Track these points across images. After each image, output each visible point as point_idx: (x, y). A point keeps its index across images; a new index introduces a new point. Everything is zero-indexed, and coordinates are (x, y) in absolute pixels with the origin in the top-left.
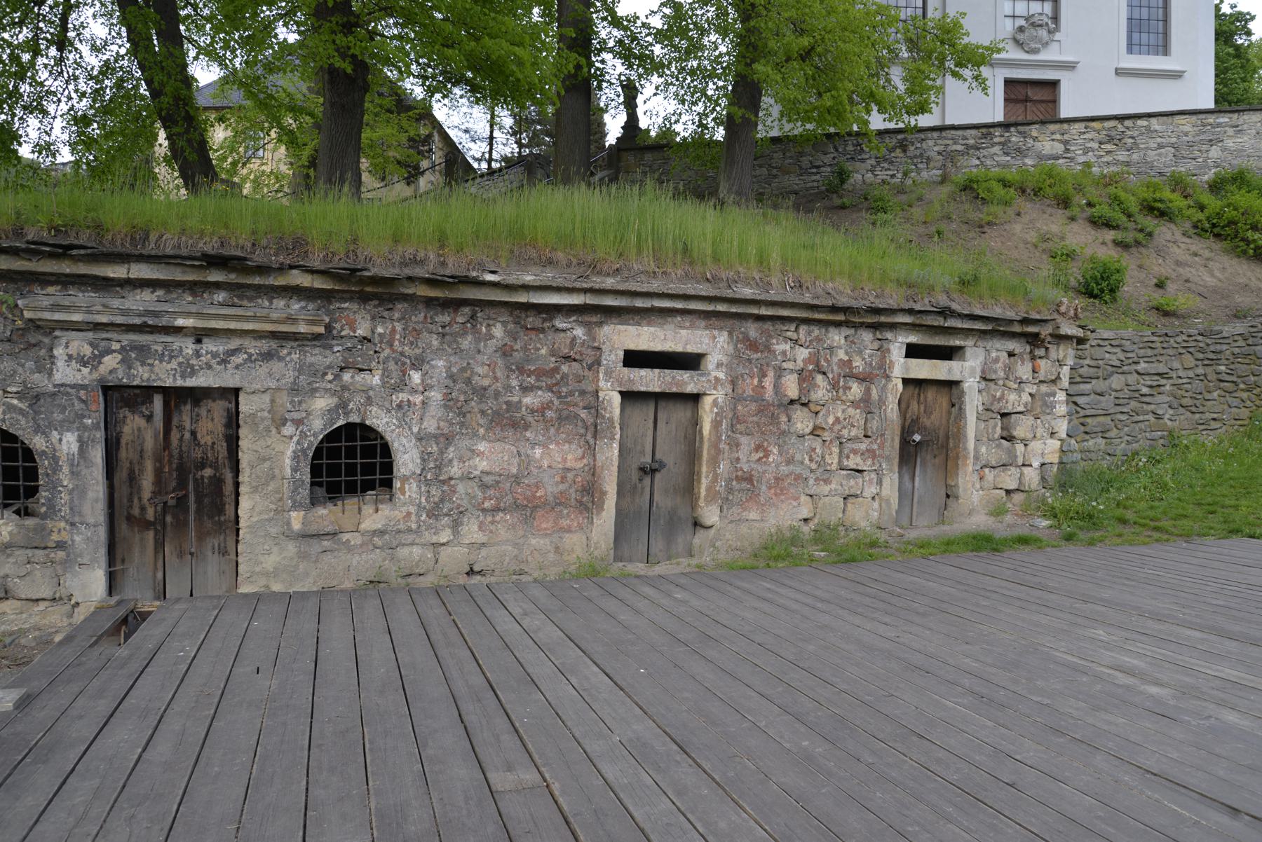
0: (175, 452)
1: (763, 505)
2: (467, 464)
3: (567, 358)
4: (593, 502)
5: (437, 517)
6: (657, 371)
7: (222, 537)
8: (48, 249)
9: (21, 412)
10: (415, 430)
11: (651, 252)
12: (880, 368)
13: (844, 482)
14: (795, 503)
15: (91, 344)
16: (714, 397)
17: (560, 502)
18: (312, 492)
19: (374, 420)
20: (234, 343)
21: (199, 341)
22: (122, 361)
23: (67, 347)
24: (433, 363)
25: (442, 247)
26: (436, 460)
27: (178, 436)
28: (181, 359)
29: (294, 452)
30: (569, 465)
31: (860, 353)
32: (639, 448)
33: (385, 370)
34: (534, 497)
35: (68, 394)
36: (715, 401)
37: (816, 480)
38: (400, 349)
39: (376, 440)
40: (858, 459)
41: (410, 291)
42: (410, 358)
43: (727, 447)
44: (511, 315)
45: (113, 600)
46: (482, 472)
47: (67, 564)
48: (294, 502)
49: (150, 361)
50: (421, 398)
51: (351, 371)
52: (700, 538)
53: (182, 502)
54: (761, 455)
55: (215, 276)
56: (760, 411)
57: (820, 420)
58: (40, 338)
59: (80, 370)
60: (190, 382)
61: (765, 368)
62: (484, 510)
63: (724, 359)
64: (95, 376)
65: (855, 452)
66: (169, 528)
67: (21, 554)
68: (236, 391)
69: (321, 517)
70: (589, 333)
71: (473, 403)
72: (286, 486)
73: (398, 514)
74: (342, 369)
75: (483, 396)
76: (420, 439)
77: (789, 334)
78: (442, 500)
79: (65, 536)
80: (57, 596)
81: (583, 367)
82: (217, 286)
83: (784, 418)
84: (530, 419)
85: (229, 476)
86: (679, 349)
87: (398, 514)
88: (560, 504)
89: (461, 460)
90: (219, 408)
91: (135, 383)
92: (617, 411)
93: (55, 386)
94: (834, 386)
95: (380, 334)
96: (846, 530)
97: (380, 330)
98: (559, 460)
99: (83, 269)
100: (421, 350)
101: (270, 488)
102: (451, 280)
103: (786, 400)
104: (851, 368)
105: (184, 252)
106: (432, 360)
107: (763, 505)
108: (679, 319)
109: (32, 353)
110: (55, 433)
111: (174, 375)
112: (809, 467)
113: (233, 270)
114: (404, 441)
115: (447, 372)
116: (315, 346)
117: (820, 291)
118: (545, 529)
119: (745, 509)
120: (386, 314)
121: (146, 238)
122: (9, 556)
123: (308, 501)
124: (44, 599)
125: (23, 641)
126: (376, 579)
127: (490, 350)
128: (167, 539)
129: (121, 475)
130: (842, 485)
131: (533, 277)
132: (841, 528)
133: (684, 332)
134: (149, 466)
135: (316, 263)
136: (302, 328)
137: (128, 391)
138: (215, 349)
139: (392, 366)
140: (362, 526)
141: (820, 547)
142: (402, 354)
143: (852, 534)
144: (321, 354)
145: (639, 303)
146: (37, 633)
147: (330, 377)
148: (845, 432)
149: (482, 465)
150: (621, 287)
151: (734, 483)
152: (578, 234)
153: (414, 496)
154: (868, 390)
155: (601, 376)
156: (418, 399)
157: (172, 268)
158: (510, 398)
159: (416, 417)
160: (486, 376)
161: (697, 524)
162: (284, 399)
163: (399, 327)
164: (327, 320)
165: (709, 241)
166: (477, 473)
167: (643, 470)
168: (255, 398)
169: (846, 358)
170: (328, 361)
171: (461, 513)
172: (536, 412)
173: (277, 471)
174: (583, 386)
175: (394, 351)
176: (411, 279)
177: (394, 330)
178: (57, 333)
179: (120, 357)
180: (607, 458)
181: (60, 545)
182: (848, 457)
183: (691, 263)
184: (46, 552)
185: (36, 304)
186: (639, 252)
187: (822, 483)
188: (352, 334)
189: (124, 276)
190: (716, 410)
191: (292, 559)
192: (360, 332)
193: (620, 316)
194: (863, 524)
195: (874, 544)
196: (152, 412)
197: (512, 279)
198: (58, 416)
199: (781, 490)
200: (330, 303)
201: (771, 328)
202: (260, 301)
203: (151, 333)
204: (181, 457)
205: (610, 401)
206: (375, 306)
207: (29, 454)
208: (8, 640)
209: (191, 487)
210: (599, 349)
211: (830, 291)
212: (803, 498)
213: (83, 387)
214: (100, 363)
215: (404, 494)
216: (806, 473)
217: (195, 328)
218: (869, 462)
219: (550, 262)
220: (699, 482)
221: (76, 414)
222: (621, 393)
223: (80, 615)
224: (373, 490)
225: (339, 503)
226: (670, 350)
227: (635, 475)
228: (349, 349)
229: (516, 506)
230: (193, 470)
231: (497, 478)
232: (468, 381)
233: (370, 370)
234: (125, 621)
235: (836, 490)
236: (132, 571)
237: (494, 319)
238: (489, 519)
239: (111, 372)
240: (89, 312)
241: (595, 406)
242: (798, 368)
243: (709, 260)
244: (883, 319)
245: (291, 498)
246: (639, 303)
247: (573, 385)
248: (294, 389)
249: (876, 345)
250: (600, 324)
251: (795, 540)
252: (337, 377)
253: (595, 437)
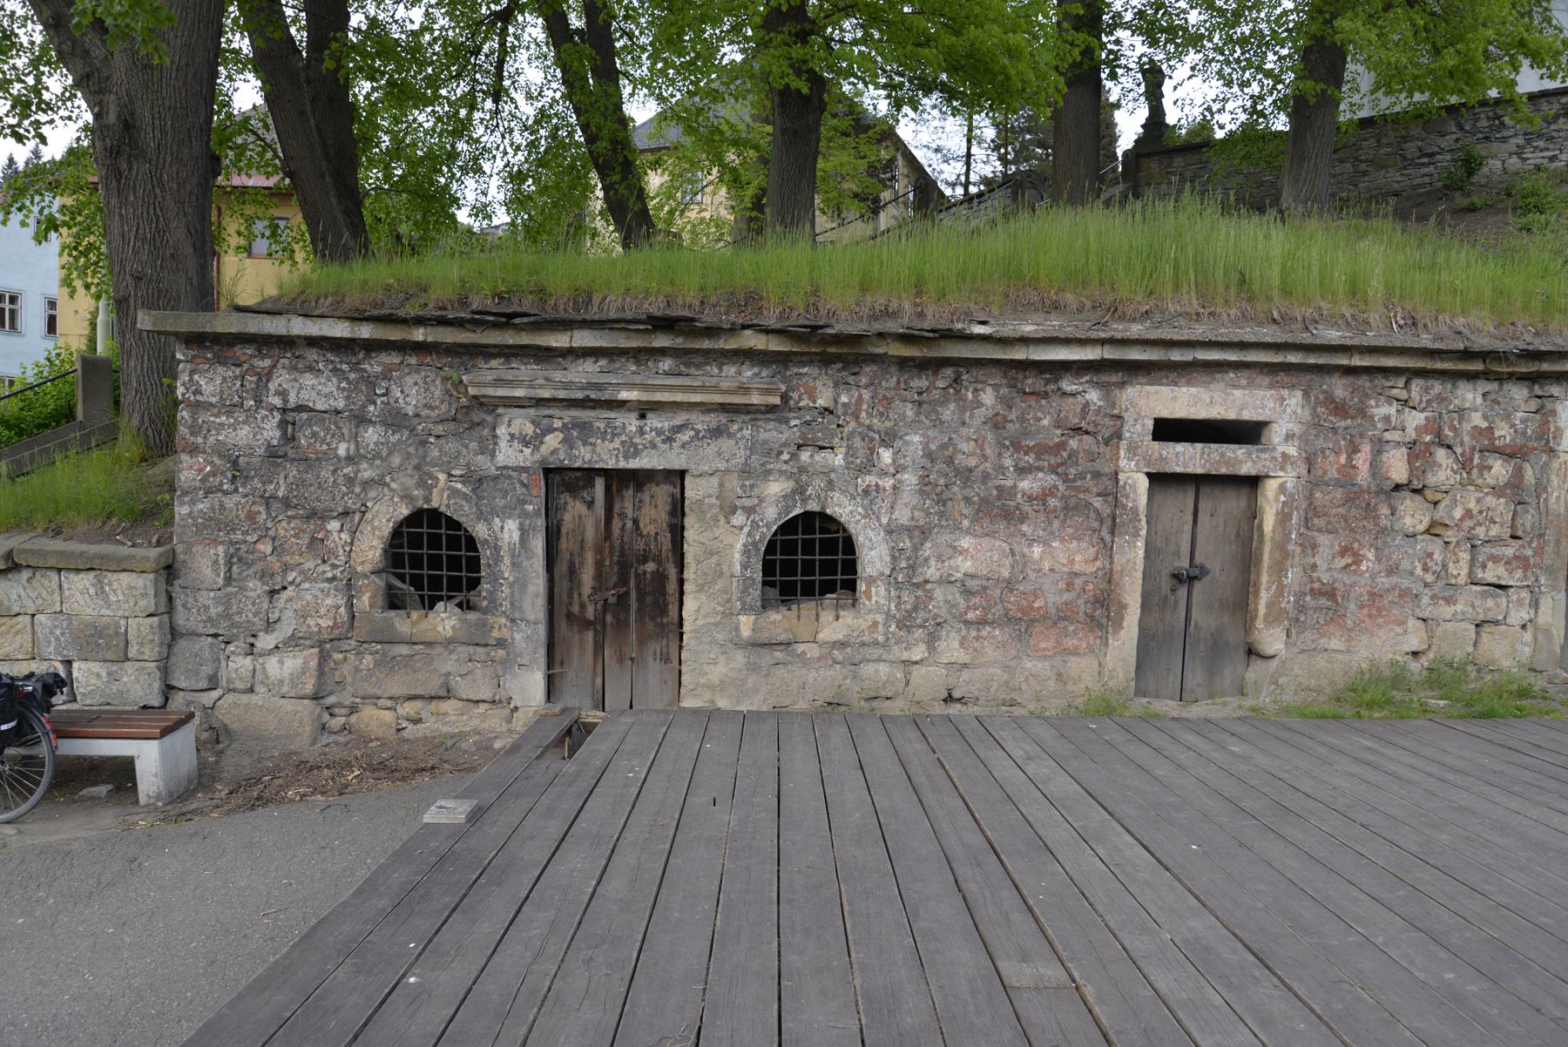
0: (617, 543)
1: (1350, 630)
2: (946, 564)
3: (1077, 430)
4: (1108, 617)
5: (909, 629)
6: (1199, 446)
7: (664, 642)
8: (492, 318)
9: (465, 497)
10: (884, 520)
11: (1193, 285)
12: (1539, 438)
13: (1477, 602)
14: (1398, 630)
15: (533, 422)
16: (1280, 481)
17: (1064, 615)
18: (762, 591)
19: (836, 509)
20: (680, 418)
21: (643, 417)
22: (564, 441)
23: (509, 426)
24: (907, 438)
25: (919, 293)
26: (909, 558)
27: (620, 525)
28: (624, 438)
29: (744, 545)
30: (1077, 568)
31: (1507, 416)
32: (1172, 548)
33: (849, 447)
34: (1032, 608)
35: (510, 477)
36: (1282, 488)
37: (1432, 598)
38: (867, 422)
39: (838, 532)
40: (1501, 570)
41: (880, 351)
42: (879, 432)
43: (1299, 549)
44: (1005, 376)
45: (557, 708)
46: (965, 575)
47: (507, 663)
48: (744, 604)
49: (592, 440)
50: (892, 481)
51: (810, 448)
52: (1255, 672)
53: (623, 599)
54: (1349, 561)
55: (662, 341)
56: (1348, 500)
57: (1441, 513)
58: (484, 416)
59: (522, 451)
60: (634, 464)
61: (1357, 440)
62: (966, 622)
63: (1297, 429)
64: (537, 457)
65: (1495, 559)
66: (609, 629)
67: (463, 651)
68: (682, 474)
69: (774, 623)
70: (1107, 397)
71: (955, 489)
72: (735, 585)
73: (863, 623)
74: (799, 447)
75: (968, 479)
76: (890, 532)
77: (1395, 392)
78: (916, 608)
79: (505, 633)
80: (497, 698)
81: (1098, 442)
82: (663, 352)
83: (1384, 510)
84: (1027, 508)
85: (672, 572)
86: (1231, 415)
87: (863, 623)
88: (1065, 618)
89: (940, 558)
90: (662, 494)
91: (576, 465)
92: (1143, 500)
93: (498, 468)
94: (1465, 465)
95: (844, 405)
96: (1479, 671)
97: (844, 399)
98: (1065, 561)
99: (525, 339)
100: (892, 422)
101: (717, 587)
102: (931, 335)
103: (1388, 485)
104: (1492, 439)
105: (629, 315)
106: (906, 434)
107: (1350, 630)
108: (1232, 375)
109: (476, 432)
110: (497, 520)
111: (617, 456)
112: (1422, 580)
113: (681, 333)
114: (871, 534)
115: (923, 449)
116: (769, 420)
117: (1445, 329)
118: (1045, 649)
119: (1323, 635)
120: (851, 379)
121: (589, 301)
122: (451, 652)
123: (759, 604)
124: (484, 701)
125: (464, 745)
126: (836, 701)
127: (977, 422)
128: (607, 641)
129: (562, 567)
130: (1473, 606)
131: (1035, 327)
132: (1470, 668)
133: (1238, 393)
134: (590, 558)
135: (772, 322)
136: (756, 399)
137: (570, 473)
138: (659, 426)
139: (858, 443)
140: (821, 636)
141: (1437, 693)
142: (870, 428)
143: (1489, 677)
144: (776, 429)
145: (1176, 356)
146: (477, 737)
147: (785, 457)
148: (1480, 531)
149: (965, 565)
150: (1152, 335)
151: (1308, 598)
152: (1093, 268)
153: (882, 601)
154: (1518, 472)
155: (1122, 453)
156: (888, 483)
157: (616, 334)
158: (1002, 482)
159: (886, 504)
160: (972, 454)
161: (1252, 652)
162: (733, 482)
163: (866, 395)
164: (783, 388)
165: (1276, 269)
166: (959, 575)
167: (1177, 577)
168: (702, 481)
169: (1485, 425)
170: (784, 437)
171: (938, 624)
172: (1036, 499)
173: (725, 568)
174: (1097, 466)
175: (860, 424)
176: (881, 335)
177: (860, 399)
178: (500, 410)
179: (561, 436)
180: (1128, 561)
181: (501, 643)
182: (1484, 567)
183: (1250, 300)
184: (487, 649)
185: (480, 379)
186: (1177, 287)
187: (1441, 602)
188: (811, 405)
189: (567, 345)
190: (1282, 498)
191: (740, 671)
192: (821, 402)
193: (1149, 374)
194: (1506, 663)
195: (1524, 693)
196: (593, 498)
197: (1007, 331)
198: (500, 502)
199: (1379, 610)
200: (787, 368)
201: (1368, 384)
202: (708, 368)
203: (594, 408)
204: (622, 549)
205: (1133, 487)
206: (839, 370)
207: (471, 543)
208: (449, 743)
209: (632, 583)
210: (1119, 417)
211: (1462, 329)
212: (1412, 622)
213: (524, 469)
214: (542, 442)
215: (869, 599)
216: (1417, 588)
217: (639, 401)
218: (1519, 574)
219: (1056, 307)
220: (1257, 594)
221: (518, 499)
222: (1148, 474)
223: (520, 723)
224: (833, 592)
225: (794, 607)
226: (1219, 417)
227: (1166, 584)
228: (808, 423)
229: (1008, 619)
230: (635, 564)
231: (985, 583)
232: (950, 461)
233: (832, 448)
234: (569, 732)
235: (1463, 613)
236: (570, 676)
237: (983, 382)
238: (974, 633)
239: (552, 452)
240: (531, 387)
241: (1113, 491)
242: (1407, 440)
243: (1276, 293)
244: (1546, 367)
245: (740, 599)
246: (1176, 356)
247: (1084, 465)
248: (746, 472)
249: (1534, 405)
250: (1122, 385)
251: (1398, 679)
252: (794, 456)
253: (1112, 533)
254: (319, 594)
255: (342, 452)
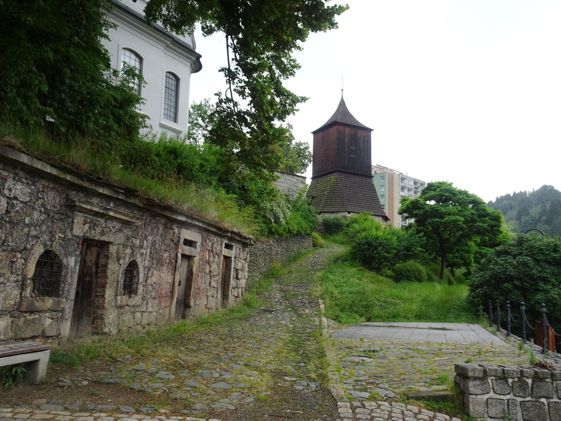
35: (73, 240)
254: (12, 288)
255: (27, 221)
